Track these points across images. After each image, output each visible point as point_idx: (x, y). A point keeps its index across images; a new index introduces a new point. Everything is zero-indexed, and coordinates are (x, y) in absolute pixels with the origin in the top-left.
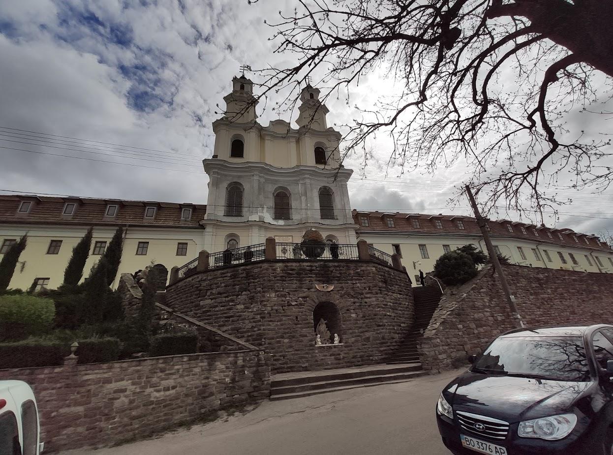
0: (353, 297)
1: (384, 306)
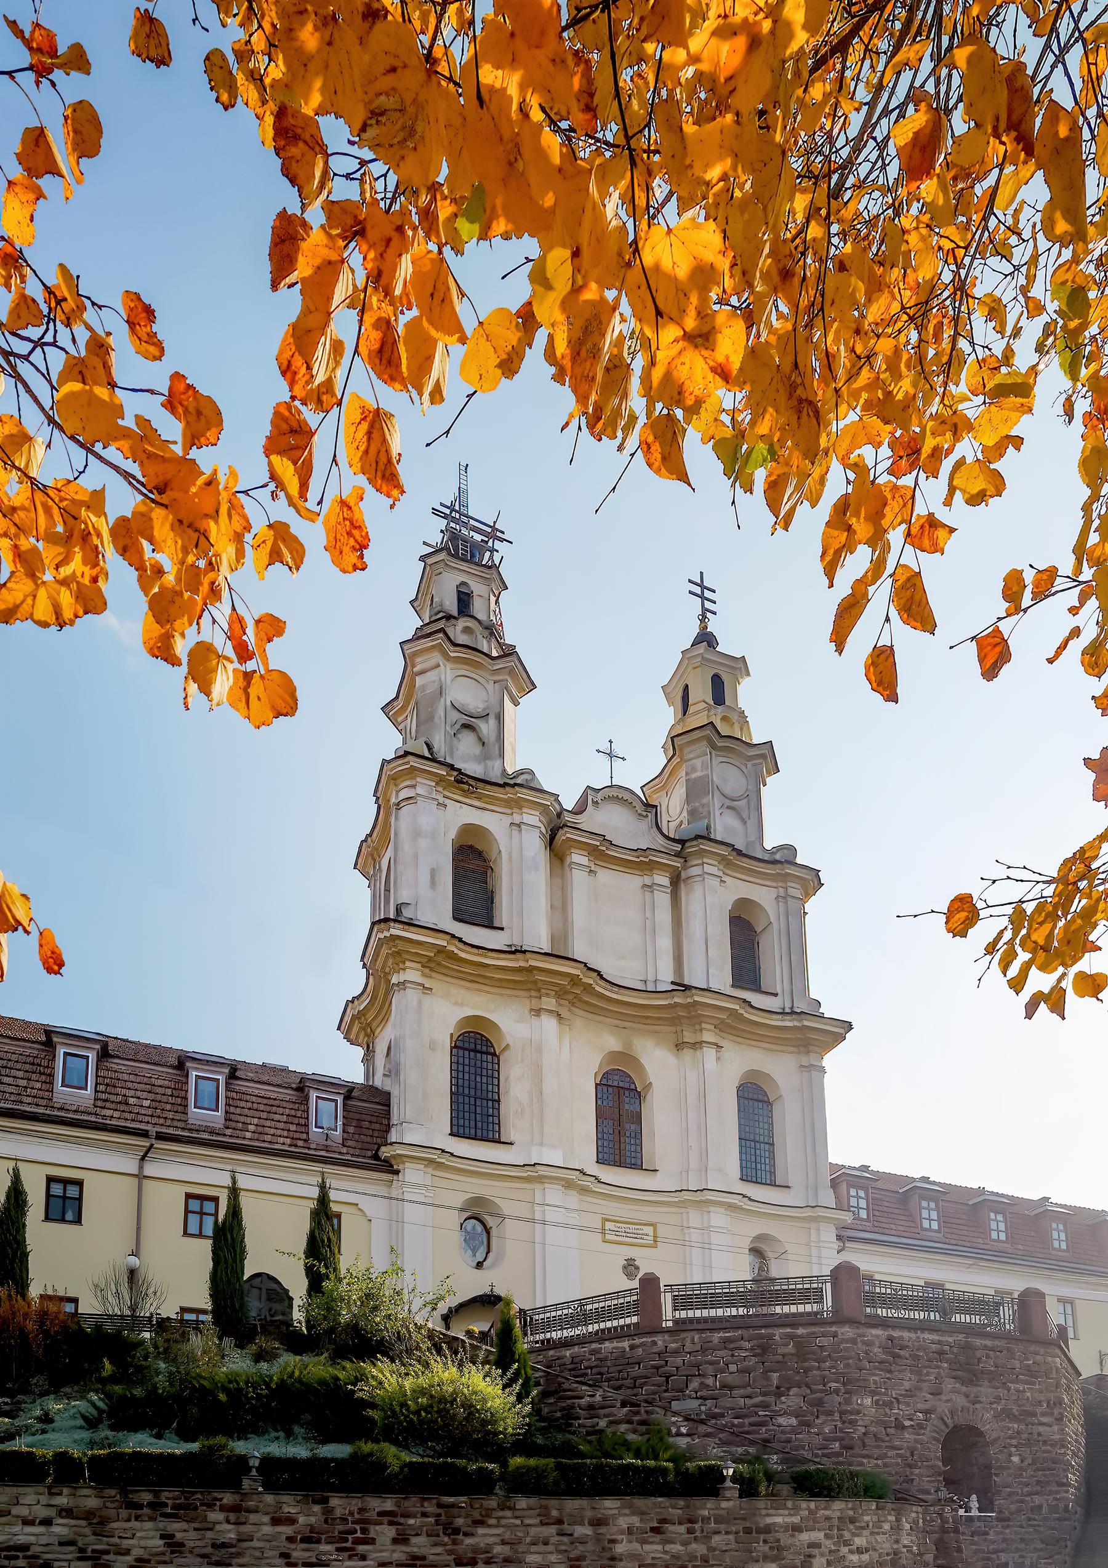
0: (1015, 1419)
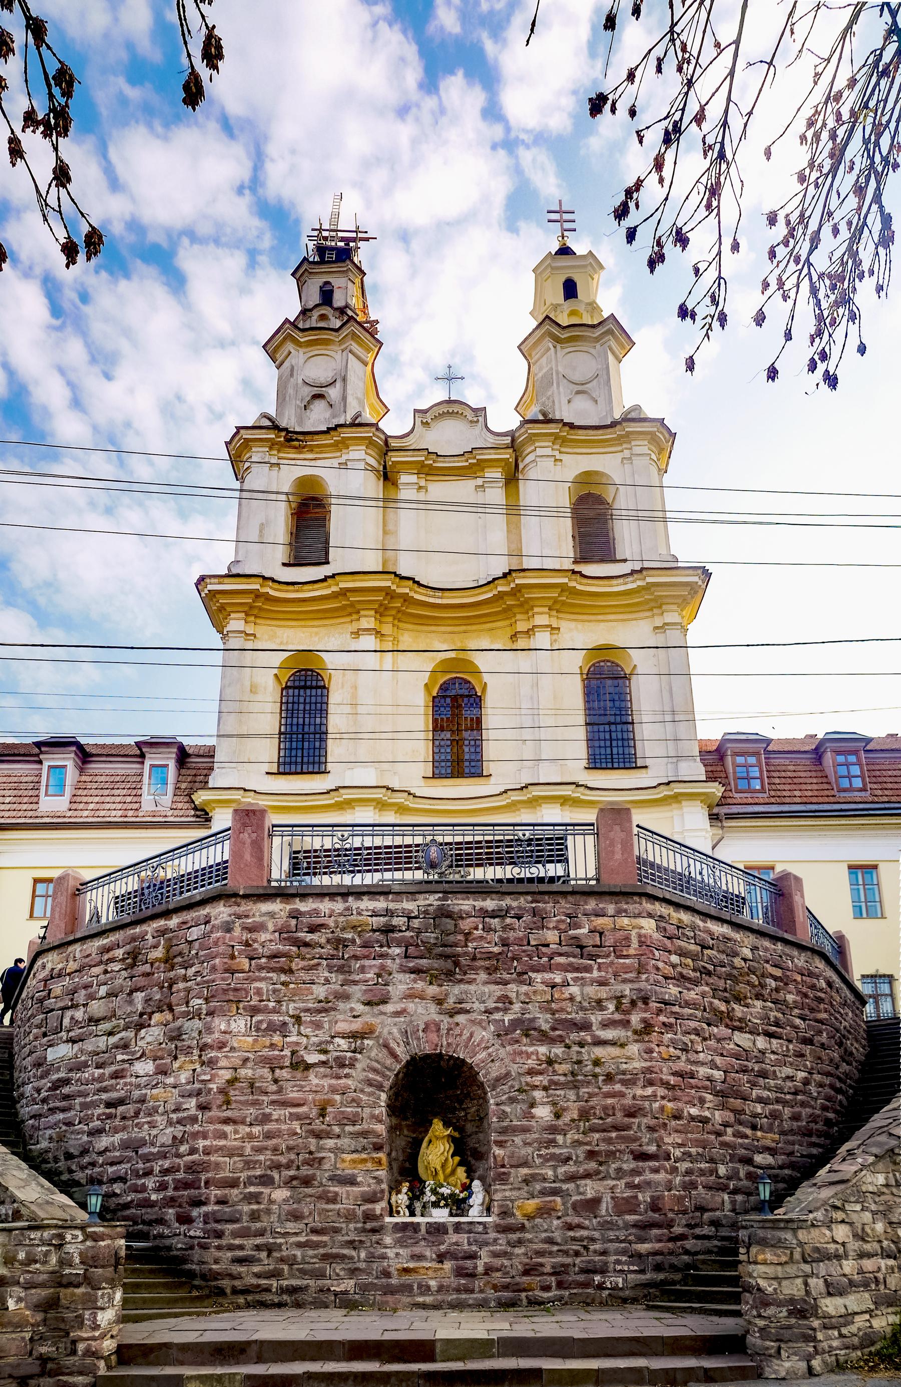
0: (545, 1038)
1: (672, 1080)
